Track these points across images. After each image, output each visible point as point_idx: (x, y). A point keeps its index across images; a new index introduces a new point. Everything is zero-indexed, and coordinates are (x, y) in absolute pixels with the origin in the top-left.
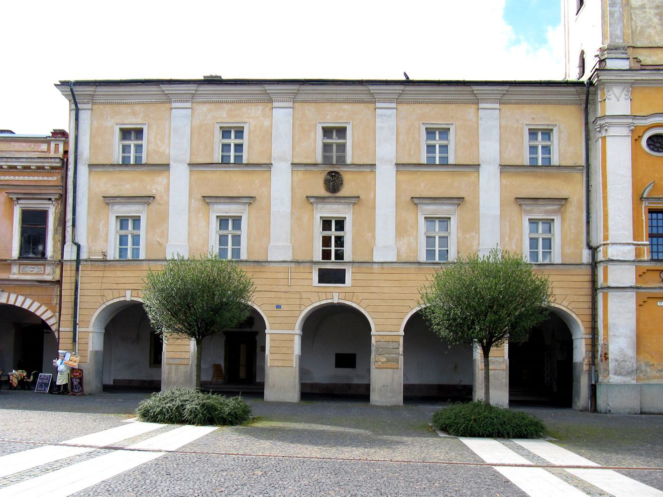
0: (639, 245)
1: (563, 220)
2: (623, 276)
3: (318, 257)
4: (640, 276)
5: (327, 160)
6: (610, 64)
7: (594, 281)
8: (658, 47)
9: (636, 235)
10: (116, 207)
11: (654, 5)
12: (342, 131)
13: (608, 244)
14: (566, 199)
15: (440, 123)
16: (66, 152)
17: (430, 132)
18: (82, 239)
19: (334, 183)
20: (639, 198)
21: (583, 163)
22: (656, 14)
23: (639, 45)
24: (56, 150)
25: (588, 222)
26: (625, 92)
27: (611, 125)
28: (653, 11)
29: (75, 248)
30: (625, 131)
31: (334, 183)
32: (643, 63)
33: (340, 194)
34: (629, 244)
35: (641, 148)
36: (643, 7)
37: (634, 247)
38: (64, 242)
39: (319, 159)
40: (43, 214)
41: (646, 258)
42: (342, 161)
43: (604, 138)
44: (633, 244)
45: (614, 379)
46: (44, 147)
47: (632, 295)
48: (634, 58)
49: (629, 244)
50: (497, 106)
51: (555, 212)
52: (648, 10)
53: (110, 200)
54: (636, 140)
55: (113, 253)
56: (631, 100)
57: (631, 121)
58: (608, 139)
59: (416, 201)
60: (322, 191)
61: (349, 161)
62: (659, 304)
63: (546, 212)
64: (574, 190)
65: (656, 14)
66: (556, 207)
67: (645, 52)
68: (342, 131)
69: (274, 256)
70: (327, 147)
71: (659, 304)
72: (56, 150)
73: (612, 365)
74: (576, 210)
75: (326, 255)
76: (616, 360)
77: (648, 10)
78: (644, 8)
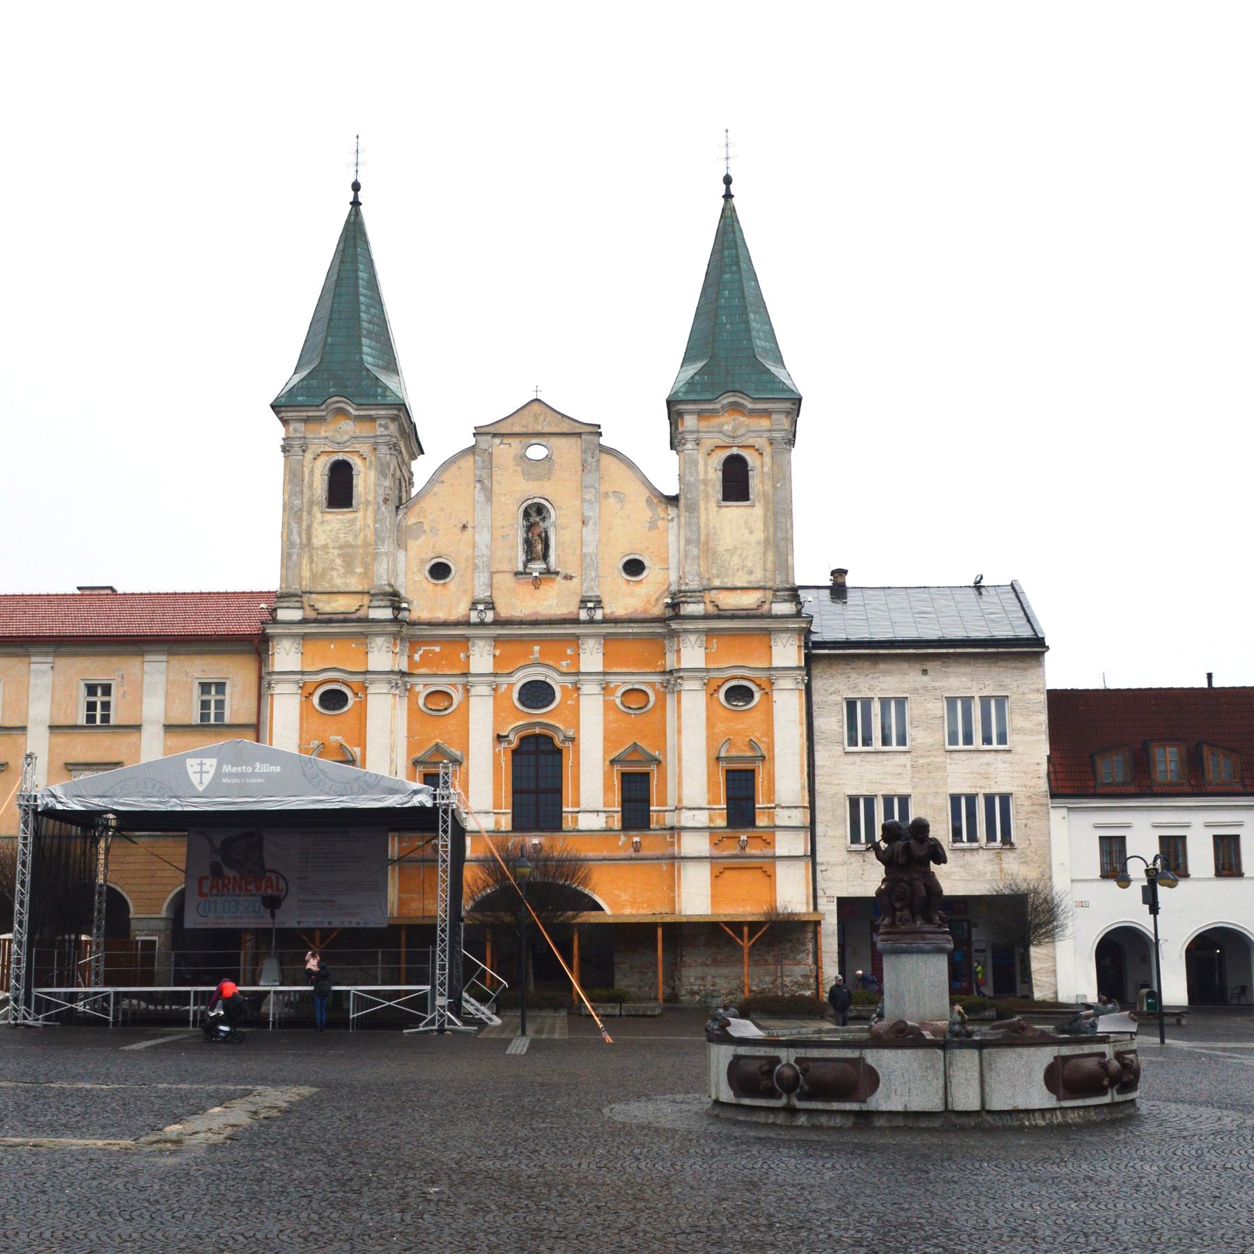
6: (282, 615)
11: (337, 545)
15: (99, 678)
17: (91, 689)
22: (339, 555)
26: (295, 646)
28: (336, 552)
30: (293, 688)
36: (325, 547)
43: (272, 695)
52: (331, 551)
59: (70, 768)
65: (339, 555)
67: (325, 597)
77: (331, 551)
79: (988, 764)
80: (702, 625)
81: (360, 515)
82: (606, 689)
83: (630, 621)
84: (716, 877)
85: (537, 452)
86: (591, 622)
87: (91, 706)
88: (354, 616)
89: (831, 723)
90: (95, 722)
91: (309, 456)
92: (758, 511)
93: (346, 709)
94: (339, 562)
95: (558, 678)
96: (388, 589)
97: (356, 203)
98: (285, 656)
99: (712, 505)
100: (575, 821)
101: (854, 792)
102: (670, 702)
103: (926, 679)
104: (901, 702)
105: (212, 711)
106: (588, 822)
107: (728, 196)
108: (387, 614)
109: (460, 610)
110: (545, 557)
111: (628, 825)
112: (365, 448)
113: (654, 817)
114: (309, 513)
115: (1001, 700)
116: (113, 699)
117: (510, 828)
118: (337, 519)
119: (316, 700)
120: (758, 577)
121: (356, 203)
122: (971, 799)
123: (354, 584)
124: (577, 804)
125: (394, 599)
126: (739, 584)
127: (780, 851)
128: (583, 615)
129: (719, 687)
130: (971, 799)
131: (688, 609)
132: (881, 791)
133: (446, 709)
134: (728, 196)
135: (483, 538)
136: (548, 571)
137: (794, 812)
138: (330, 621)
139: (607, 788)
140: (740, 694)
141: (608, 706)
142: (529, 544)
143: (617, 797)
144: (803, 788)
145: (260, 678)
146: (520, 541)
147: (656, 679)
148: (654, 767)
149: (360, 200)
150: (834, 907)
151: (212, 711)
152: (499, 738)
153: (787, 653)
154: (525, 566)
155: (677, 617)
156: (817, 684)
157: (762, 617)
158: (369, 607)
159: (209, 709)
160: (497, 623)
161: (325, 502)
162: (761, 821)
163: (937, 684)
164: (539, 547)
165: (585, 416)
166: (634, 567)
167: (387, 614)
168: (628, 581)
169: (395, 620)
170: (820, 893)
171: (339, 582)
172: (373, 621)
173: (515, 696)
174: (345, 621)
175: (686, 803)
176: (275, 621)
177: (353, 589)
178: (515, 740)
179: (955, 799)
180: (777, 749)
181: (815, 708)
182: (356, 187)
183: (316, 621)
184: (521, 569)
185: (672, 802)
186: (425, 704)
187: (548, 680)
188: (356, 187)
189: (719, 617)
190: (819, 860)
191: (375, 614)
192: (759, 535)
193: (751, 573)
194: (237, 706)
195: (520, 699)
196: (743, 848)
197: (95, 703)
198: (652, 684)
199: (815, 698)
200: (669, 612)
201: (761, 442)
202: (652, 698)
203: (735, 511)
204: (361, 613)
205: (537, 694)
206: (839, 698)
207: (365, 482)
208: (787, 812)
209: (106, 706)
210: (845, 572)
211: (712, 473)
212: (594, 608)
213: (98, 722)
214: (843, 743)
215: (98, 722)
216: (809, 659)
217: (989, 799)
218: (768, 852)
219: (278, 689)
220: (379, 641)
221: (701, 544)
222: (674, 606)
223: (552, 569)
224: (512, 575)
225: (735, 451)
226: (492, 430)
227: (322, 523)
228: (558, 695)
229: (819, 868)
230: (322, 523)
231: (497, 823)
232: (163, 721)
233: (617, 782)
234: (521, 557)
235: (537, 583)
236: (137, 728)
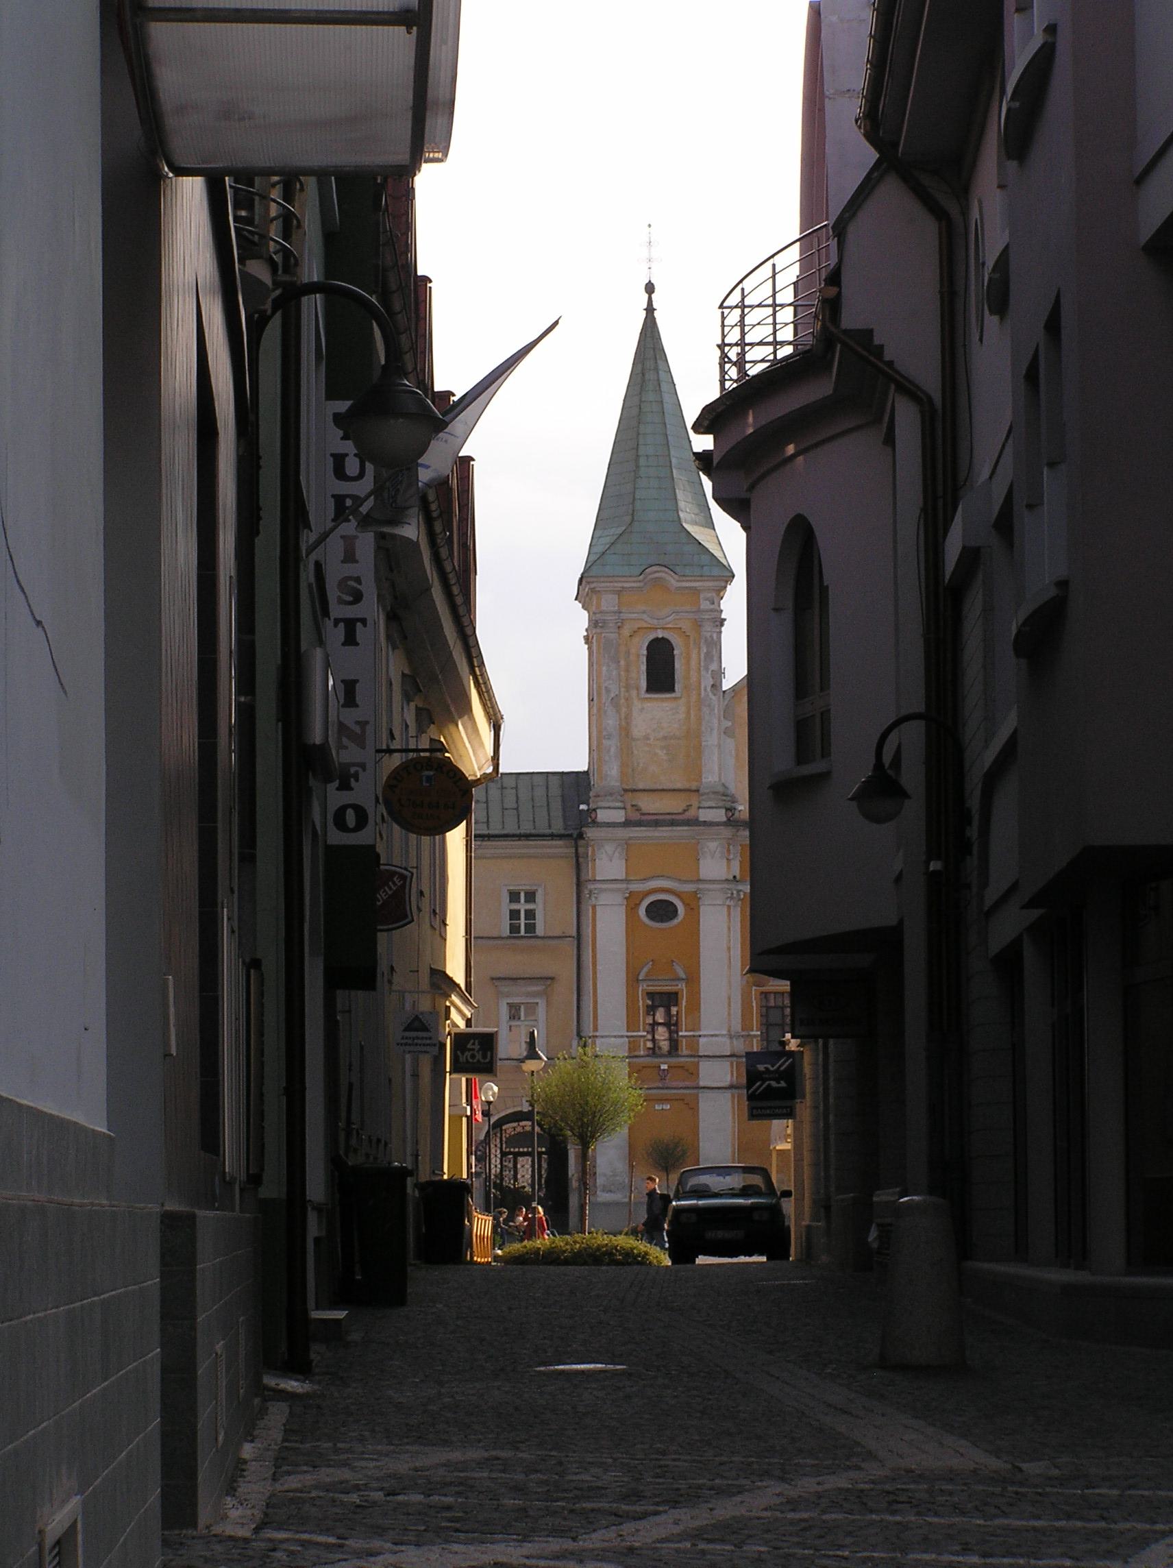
0: (632, 1036)
1: (548, 1004)
8: (663, 790)
9: (632, 1024)
13: (596, 1036)
14: (552, 979)
20: (633, 980)
21: (574, 933)
23: (641, 786)
25: (578, 1008)
27: (602, 890)
30: (619, 899)
32: (645, 810)
34: (622, 1036)
35: (638, 916)
36: (647, 738)
37: (627, 1039)
43: (594, 907)
44: (627, 1037)
45: (603, 1197)
48: (633, 806)
49: (622, 1036)
54: (632, 909)
56: (626, 860)
57: (624, 886)
58: (598, 908)
62: (657, 1108)
63: (529, 994)
64: (566, 972)
65: (662, 748)
66: (539, 988)
71: (657, 1108)
73: (600, 1181)
76: (605, 1175)
78: (648, 739)
87: (514, 915)
88: (681, 817)
90: (519, 932)
91: (626, 632)
93: (675, 922)
96: (721, 789)
116: (538, 907)
119: (642, 911)
138: (656, 824)
145: (579, 884)
149: (655, 307)
151: (523, 921)
158: (699, 808)
159: (519, 919)
161: (644, 684)
172: (705, 823)
174: (673, 823)
176: (595, 823)
177: (679, 786)
191: (705, 815)
197: (519, 911)
204: (691, 813)
209: (530, 914)
213: (522, 932)
215: (522, 932)
219: (604, 899)
220: (713, 845)
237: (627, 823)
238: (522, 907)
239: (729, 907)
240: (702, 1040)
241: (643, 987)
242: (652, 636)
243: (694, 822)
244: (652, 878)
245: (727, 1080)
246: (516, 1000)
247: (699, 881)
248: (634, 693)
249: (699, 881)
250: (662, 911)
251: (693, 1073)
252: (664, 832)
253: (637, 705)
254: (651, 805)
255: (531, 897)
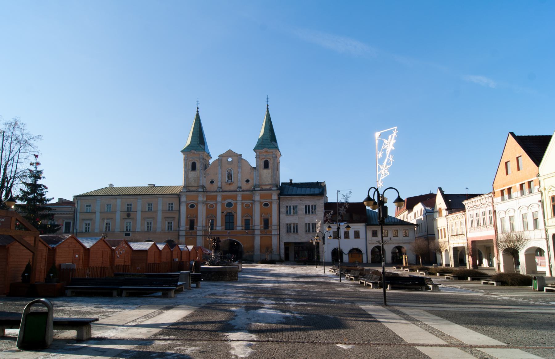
1: (174, 222)
2: (183, 233)
3: (125, 230)
4: (187, 233)
5: (128, 211)
7: (179, 234)
10: (85, 221)
12: (131, 205)
14: (175, 217)
16: (75, 210)
18: (78, 228)
19: (129, 215)
20: (187, 217)
24: (73, 209)
28: (193, 179)
29: (76, 230)
31: (129, 215)
33: (130, 218)
36: (191, 178)
38: (74, 229)
39: (126, 210)
40: (70, 223)
41: (188, 229)
42: (131, 211)
46: (70, 209)
47: (184, 237)
50: (162, 199)
51: (172, 220)
53: (83, 220)
54: (187, 206)
55: (84, 231)
60: (126, 217)
61: (132, 211)
68: (131, 205)
69: (116, 231)
70: (128, 208)
72: (73, 209)
74: (177, 220)
75: (127, 230)
79: (312, 217)
80: (259, 192)
81: (197, 172)
82: (242, 204)
83: (247, 191)
84: (261, 238)
85: (230, 160)
86: (240, 191)
89: (283, 210)
91: (188, 161)
92: (270, 170)
94: (193, 181)
95: (233, 201)
97: (198, 112)
98: (183, 199)
99: (262, 169)
100: (236, 228)
101: (287, 223)
102: (254, 206)
103: (301, 201)
104: (296, 206)
105: (171, 208)
106: (239, 228)
107: (268, 109)
108: (202, 190)
109: (216, 189)
110: (231, 179)
111: (246, 229)
112: (198, 160)
113: (250, 227)
114: (188, 171)
115: (315, 206)
117: (224, 229)
118: (193, 172)
120: (270, 183)
121: (198, 112)
122: (309, 224)
123: (196, 185)
124: (236, 225)
125: (203, 187)
126: (266, 184)
127: (273, 234)
128: (238, 190)
129: (262, 203)
130: (309, 224)
131: (256, 189)
132: (292, 222)
133: (213, 207)
134: (268, 109)
135: (220, 176)
136: (232, 182)
137: (275, 227)
138: (191, 192)
139: (242, 222)
140: (266, 205)
141: (242, 207)
142: (228, 177)
143: (244, 223)
144: (277, 222)
145: (179, 202)
146: (227, 177)
147: (251, 202)
148: (250, 218)
150: (283, 244)
151: (171, 208)
152: (222, 213)
153: (275, 197)
154: (228, 181)
155: (255, 190)
156: (280, 203)
157: (270, 190)
160: (222, 192)
161: (191, 169)
162: (270, 228)
163: (303, 202)
164: (230, 178)
165: (239, 153)
166: (247, 181)
167: (202, 190)
168: (247, 184)
169: (203, 191)
170: (281, 241)
171: (193, 185)
172: (199, 192)
173: (226, 205)
175: (256, 225)
178: (225, 213)
179: (306, 224)
180: (273, 215)
181: (280, 207)
182: (198, 108)
183: (189, 192)
184: (227, 181)
185: (254, 224)
186: (209, 207)
187: (232, 202)
188: (198, 108)
189: (262, 190)
190: (281, 235)
192: (270, 175)
193: (269, 182)
194: (175, 207)
195: (226, 206)
196: (266, 233)
198: (250, 203)
199: (280, 205)
200: (254, 190)
201: (271, 157)
202: (250, 205)
203: (266, 171)
204: (197, 190)
205: (229, 205)
206: (285, 205)
207: (198, 166)
208: (274, 227)
210: (292, 180)
211: (262, 164)
212: (240, 189)
214: (285, 213)
216: (279, 198)
217: (313, 224)
218: (271, 234)
220: (200, 195)
221: (260, 176)
222: (254, 188)
223: (233, 181)
224: (225, 183)
225: (266, 159)
226: (222, 155)
227: (190, 173)
228: (233, 205)
229: (281, 237)
230: (190, 173)
231: (222, 228)
232: (161, 210)
233: (244, 221)
234: (227, 179)
235: (229, 184)
236: (157, 211)
237: (187, 192)
238: (150, 206)
239: (203, 205)
240: (198, 228)
241: (189, 219)
242: (192, 161)
243: (198, 191)
244: (190, 201)
245: (202, 234)
246: (169, 221)
247: (198, 201)
248: (189, 171)
249: (198, 201)
250: (192, 206)
251: (196, 233)
252: (192, 193)
253: (190, 172)
254: (191, 189)
255: (172, 204)
